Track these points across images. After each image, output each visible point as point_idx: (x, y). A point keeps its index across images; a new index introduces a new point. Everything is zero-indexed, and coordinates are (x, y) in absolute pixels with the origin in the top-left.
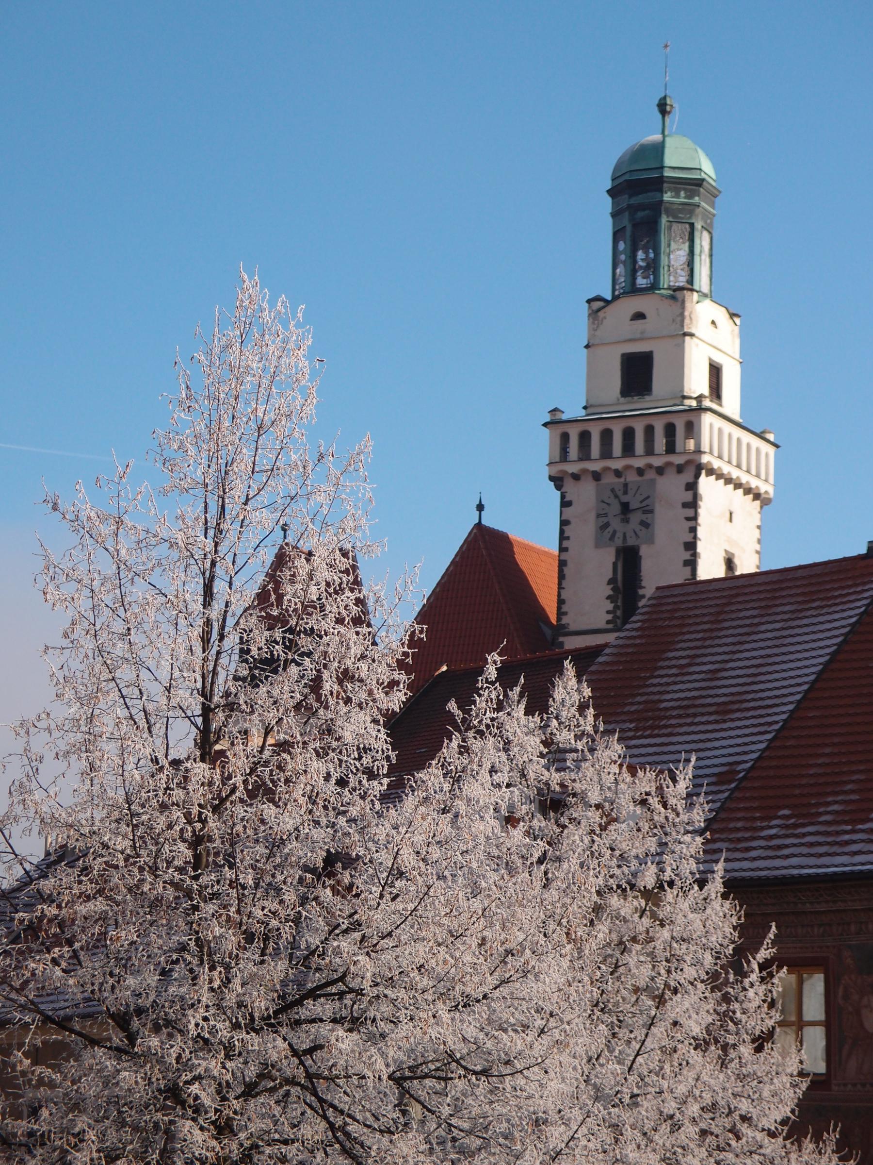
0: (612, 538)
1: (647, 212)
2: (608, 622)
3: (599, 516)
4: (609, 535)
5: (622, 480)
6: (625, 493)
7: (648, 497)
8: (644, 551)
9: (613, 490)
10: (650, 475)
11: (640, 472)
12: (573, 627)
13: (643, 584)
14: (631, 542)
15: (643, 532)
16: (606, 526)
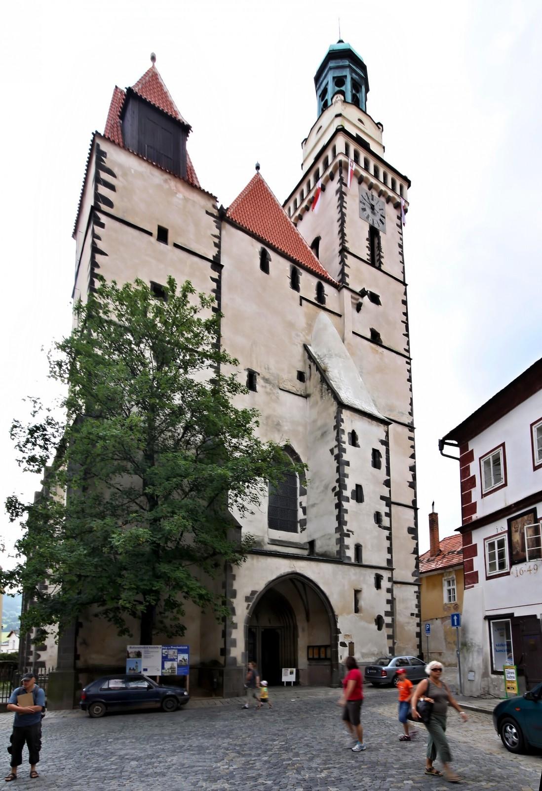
0: (368, 217)
1: (357, 77)
2: (368, 259)
3: (361, 202)
4: (366, 216)
5: (370, 192)
6: (373, 199)
7: (382, 209)
8: (381, 234)
9: (367, 194)
10: (383, 199)
11: (381, 193)
12: (350, 250)
13: (382, 251)
14: (376, 226)
15: (381, 225)
16: (364, 210)
